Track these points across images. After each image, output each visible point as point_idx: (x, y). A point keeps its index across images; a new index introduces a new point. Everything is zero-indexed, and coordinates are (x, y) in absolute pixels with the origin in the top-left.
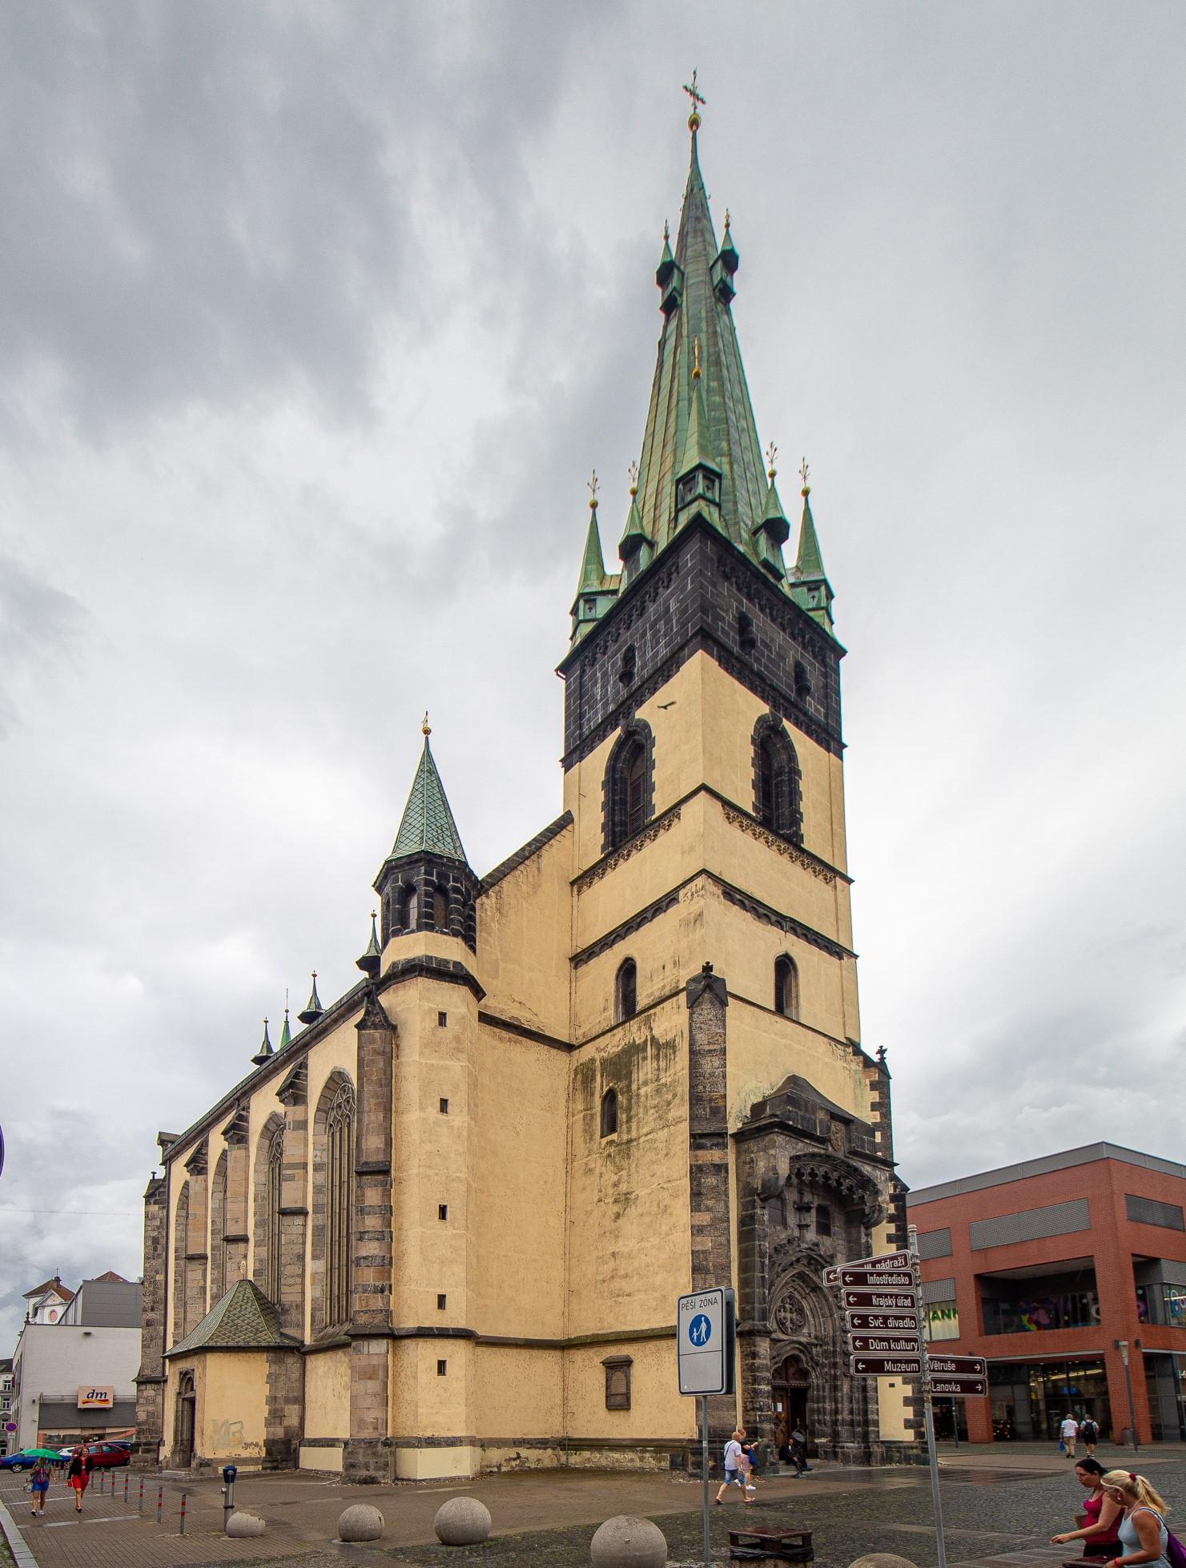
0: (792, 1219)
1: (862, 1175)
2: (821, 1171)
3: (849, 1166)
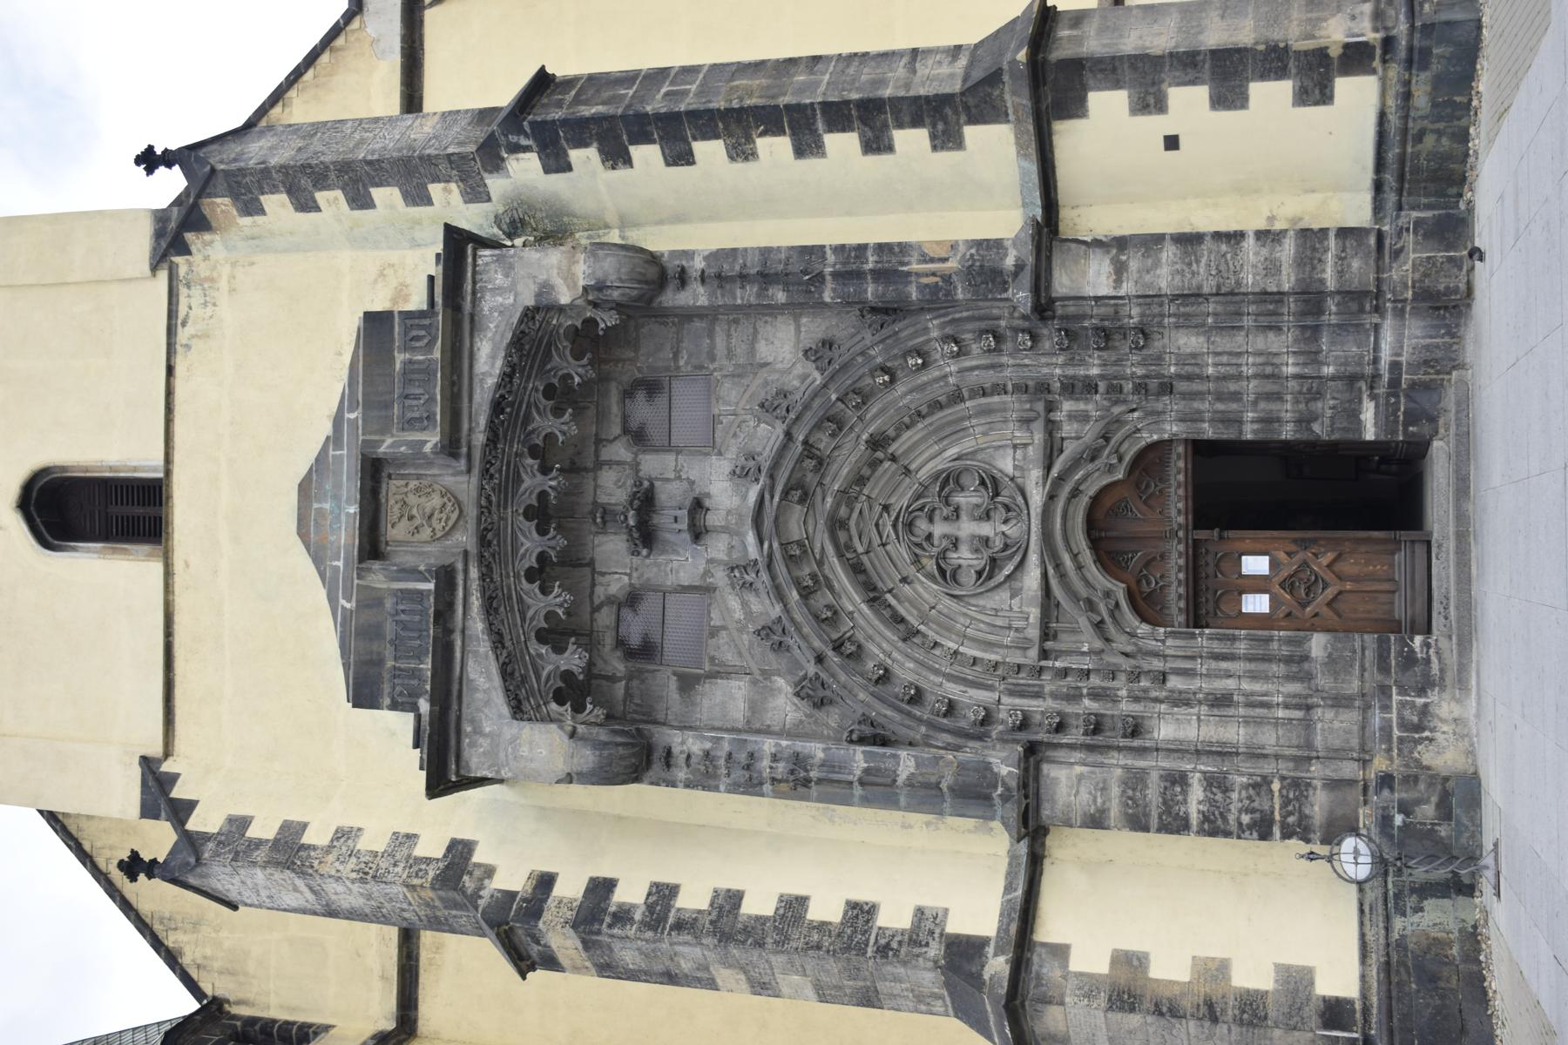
0: (681, 564)
1: (507, 377)
2: (530, 544)
3: (493, 440)
